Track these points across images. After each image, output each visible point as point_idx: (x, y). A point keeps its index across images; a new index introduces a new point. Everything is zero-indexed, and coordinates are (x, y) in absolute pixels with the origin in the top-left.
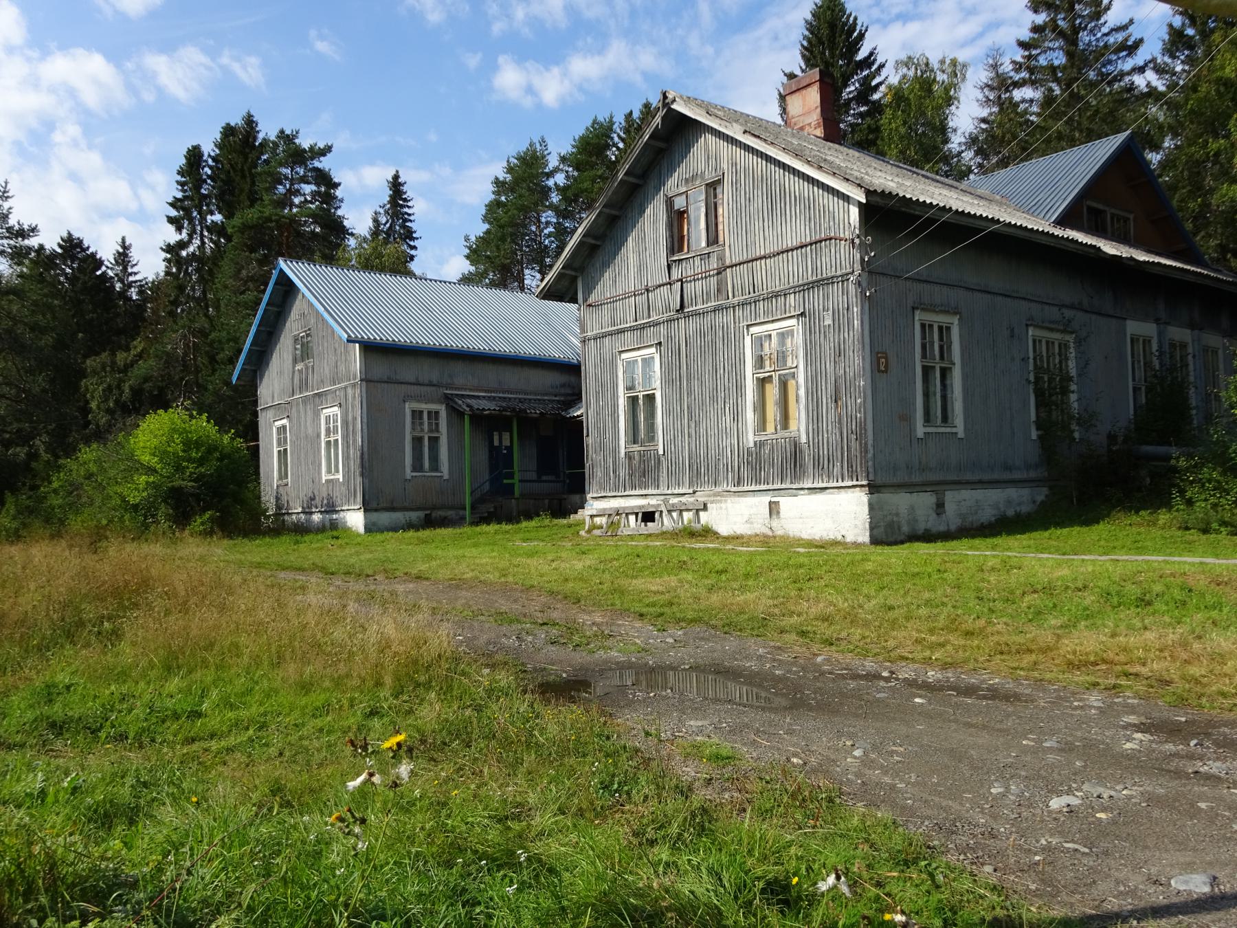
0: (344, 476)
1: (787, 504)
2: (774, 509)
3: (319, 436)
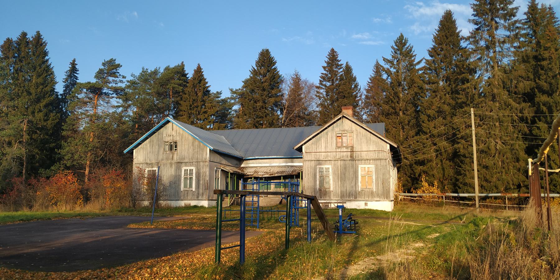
0: (195, 189)
1: (369, 203)
2: (366, 204)
3: (180, 176)
